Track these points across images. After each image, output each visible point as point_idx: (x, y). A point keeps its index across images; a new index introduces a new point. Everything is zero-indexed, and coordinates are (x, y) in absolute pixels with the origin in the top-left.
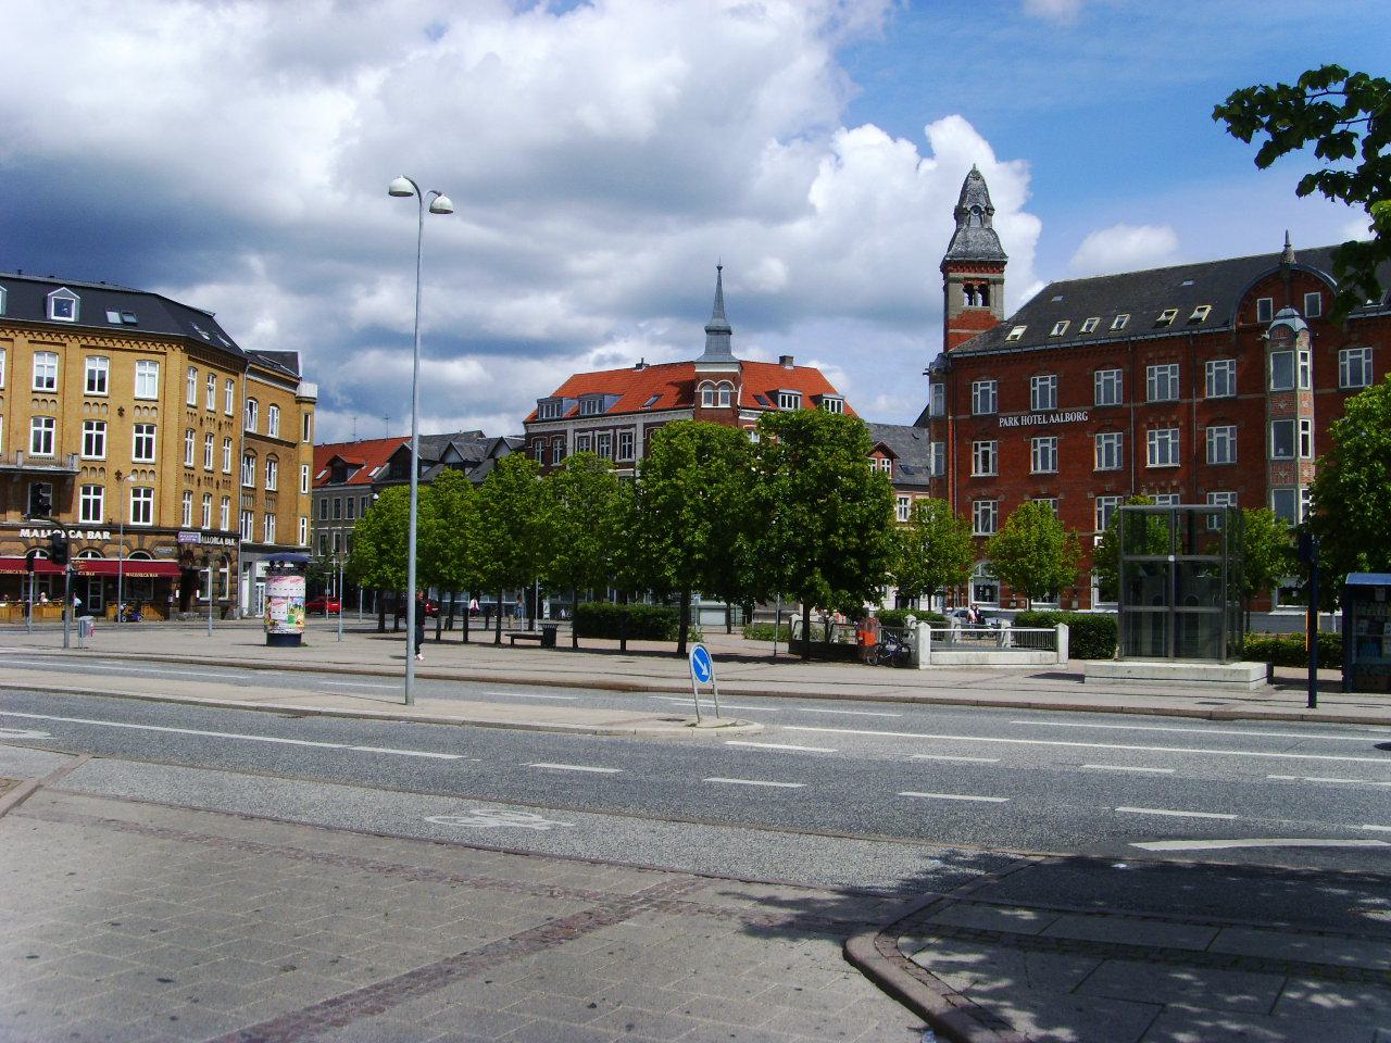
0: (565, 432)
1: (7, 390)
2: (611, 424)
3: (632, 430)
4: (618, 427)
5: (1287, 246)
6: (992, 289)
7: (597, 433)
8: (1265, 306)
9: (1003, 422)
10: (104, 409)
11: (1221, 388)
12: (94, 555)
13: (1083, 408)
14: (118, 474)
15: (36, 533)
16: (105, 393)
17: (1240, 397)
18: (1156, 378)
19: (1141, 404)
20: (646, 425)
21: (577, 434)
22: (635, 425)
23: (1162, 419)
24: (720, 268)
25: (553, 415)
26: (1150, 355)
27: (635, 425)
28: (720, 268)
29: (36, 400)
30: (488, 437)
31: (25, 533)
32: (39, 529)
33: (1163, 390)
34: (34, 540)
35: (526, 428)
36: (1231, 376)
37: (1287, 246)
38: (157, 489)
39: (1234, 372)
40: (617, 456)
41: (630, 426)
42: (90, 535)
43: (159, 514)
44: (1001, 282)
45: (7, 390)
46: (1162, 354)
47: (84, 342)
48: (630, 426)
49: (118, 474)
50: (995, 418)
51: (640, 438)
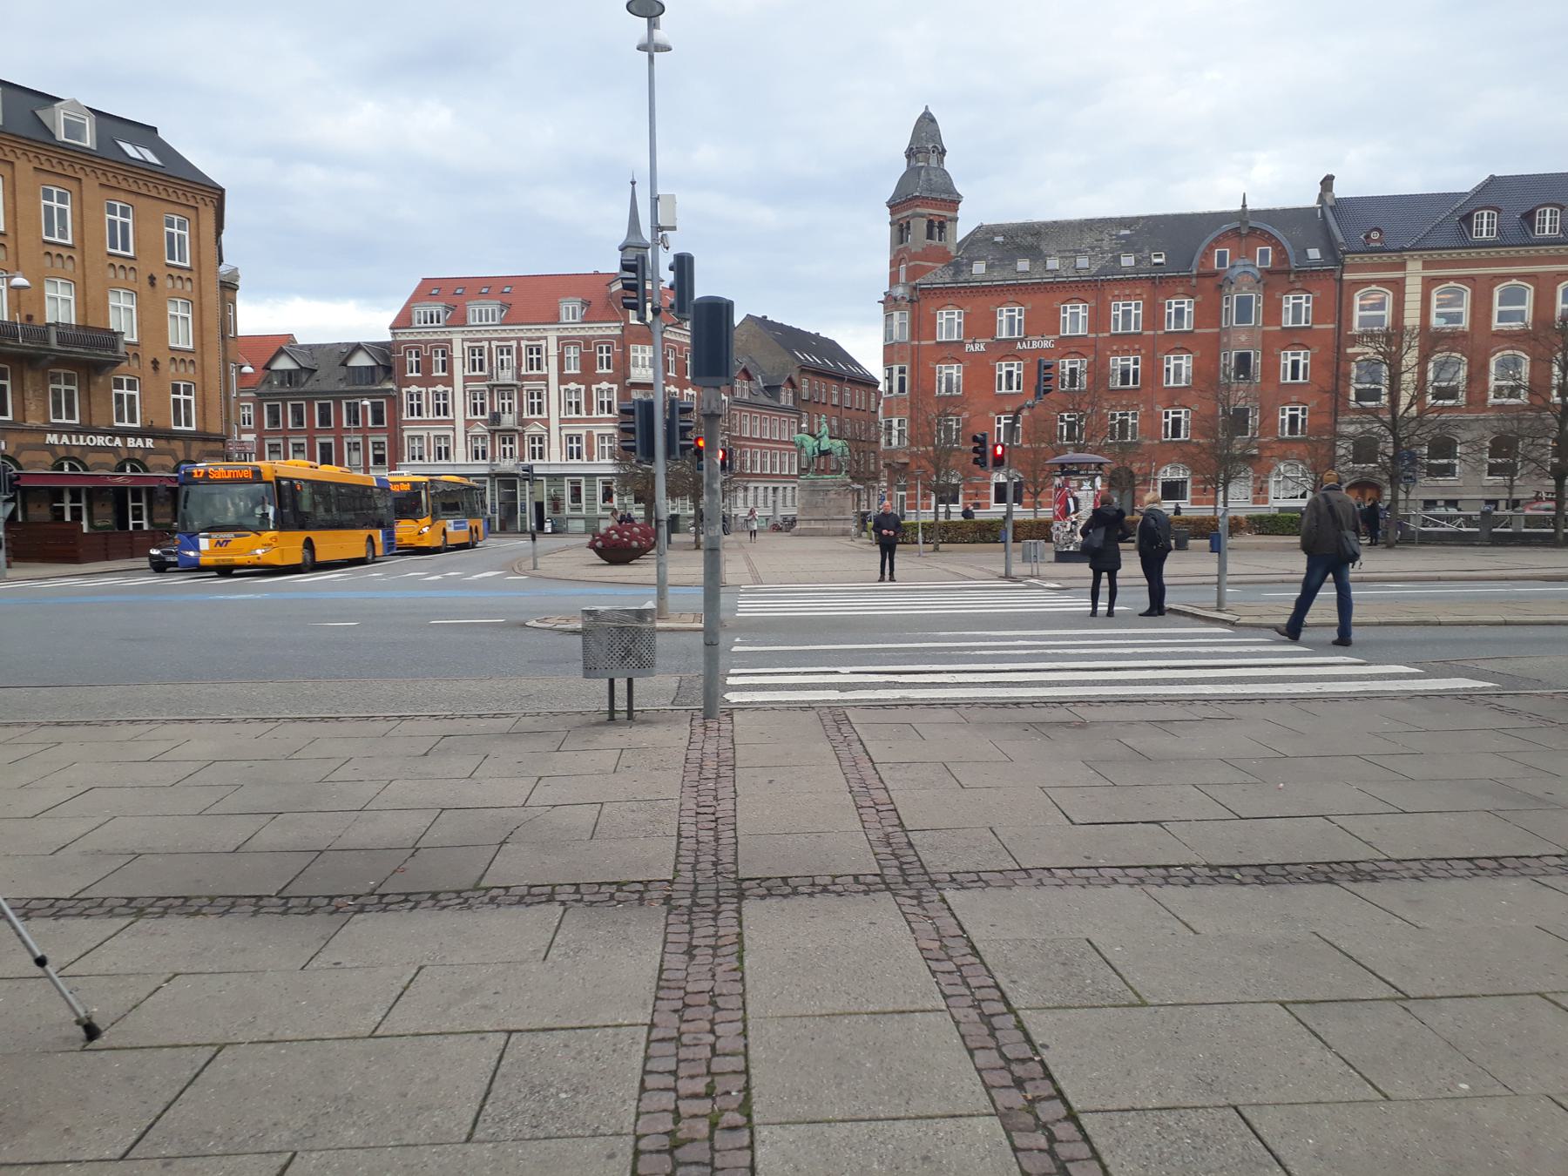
0: (450, 341)
1: (11, 234)
2: (512, 335)
3: (543, 342)
4: (522, 338)
5: (1244, 206)
6: (948, 225)
7: (494, 344)
8: (1222, 256)
9: (969, 347)
10: (131, 276)
11: (1296, 318)
12: (134, 469)
13: (1050, 337)
14: (155, 363)
15: (65, 439)
16: (131, 254)
17: (1197, 331)
18: (1120, 313)
19: (1160, 332)
20: (559, 339)
21: (467, 344)
22: (546, 338)
23: (1126, 347)
24: (633, 183)
25: (487, 320)
26: (1116, 293)
27: (546, 338)
28: (633, 183)
29: (48, 253)
30: (300, 343)
31: (52, 439)
32: (69, 434)
33: (950, 331)
34: (63, 449)
35: (394, 334)
36: (959, 324)
37: (1244, 206)
38: (199, 384)
39: (1191, 310)
40: (523, 368)
41: (539, 339)
42: (131, 442)
43: (203, 416)
44: (956, 219)
45: (11, 234)
46: (1127, 292)
47: (104, 180)
48: (539, 339)
49: (155, 363)
50: (961, 344)
51: (553, 351)
